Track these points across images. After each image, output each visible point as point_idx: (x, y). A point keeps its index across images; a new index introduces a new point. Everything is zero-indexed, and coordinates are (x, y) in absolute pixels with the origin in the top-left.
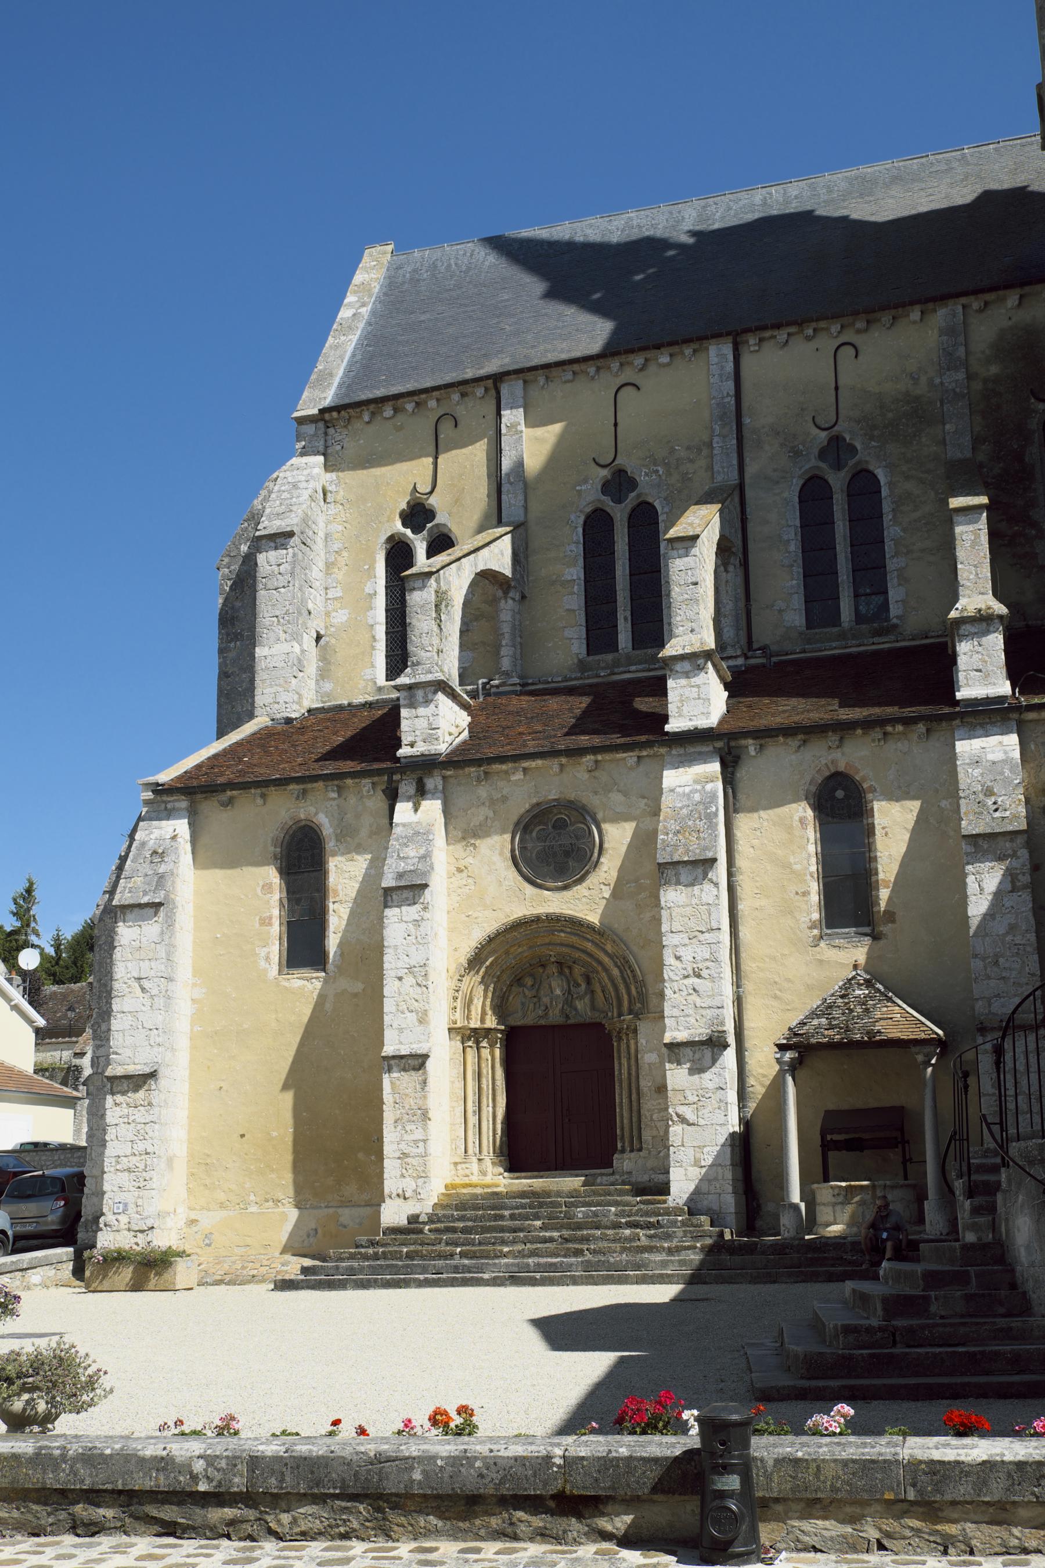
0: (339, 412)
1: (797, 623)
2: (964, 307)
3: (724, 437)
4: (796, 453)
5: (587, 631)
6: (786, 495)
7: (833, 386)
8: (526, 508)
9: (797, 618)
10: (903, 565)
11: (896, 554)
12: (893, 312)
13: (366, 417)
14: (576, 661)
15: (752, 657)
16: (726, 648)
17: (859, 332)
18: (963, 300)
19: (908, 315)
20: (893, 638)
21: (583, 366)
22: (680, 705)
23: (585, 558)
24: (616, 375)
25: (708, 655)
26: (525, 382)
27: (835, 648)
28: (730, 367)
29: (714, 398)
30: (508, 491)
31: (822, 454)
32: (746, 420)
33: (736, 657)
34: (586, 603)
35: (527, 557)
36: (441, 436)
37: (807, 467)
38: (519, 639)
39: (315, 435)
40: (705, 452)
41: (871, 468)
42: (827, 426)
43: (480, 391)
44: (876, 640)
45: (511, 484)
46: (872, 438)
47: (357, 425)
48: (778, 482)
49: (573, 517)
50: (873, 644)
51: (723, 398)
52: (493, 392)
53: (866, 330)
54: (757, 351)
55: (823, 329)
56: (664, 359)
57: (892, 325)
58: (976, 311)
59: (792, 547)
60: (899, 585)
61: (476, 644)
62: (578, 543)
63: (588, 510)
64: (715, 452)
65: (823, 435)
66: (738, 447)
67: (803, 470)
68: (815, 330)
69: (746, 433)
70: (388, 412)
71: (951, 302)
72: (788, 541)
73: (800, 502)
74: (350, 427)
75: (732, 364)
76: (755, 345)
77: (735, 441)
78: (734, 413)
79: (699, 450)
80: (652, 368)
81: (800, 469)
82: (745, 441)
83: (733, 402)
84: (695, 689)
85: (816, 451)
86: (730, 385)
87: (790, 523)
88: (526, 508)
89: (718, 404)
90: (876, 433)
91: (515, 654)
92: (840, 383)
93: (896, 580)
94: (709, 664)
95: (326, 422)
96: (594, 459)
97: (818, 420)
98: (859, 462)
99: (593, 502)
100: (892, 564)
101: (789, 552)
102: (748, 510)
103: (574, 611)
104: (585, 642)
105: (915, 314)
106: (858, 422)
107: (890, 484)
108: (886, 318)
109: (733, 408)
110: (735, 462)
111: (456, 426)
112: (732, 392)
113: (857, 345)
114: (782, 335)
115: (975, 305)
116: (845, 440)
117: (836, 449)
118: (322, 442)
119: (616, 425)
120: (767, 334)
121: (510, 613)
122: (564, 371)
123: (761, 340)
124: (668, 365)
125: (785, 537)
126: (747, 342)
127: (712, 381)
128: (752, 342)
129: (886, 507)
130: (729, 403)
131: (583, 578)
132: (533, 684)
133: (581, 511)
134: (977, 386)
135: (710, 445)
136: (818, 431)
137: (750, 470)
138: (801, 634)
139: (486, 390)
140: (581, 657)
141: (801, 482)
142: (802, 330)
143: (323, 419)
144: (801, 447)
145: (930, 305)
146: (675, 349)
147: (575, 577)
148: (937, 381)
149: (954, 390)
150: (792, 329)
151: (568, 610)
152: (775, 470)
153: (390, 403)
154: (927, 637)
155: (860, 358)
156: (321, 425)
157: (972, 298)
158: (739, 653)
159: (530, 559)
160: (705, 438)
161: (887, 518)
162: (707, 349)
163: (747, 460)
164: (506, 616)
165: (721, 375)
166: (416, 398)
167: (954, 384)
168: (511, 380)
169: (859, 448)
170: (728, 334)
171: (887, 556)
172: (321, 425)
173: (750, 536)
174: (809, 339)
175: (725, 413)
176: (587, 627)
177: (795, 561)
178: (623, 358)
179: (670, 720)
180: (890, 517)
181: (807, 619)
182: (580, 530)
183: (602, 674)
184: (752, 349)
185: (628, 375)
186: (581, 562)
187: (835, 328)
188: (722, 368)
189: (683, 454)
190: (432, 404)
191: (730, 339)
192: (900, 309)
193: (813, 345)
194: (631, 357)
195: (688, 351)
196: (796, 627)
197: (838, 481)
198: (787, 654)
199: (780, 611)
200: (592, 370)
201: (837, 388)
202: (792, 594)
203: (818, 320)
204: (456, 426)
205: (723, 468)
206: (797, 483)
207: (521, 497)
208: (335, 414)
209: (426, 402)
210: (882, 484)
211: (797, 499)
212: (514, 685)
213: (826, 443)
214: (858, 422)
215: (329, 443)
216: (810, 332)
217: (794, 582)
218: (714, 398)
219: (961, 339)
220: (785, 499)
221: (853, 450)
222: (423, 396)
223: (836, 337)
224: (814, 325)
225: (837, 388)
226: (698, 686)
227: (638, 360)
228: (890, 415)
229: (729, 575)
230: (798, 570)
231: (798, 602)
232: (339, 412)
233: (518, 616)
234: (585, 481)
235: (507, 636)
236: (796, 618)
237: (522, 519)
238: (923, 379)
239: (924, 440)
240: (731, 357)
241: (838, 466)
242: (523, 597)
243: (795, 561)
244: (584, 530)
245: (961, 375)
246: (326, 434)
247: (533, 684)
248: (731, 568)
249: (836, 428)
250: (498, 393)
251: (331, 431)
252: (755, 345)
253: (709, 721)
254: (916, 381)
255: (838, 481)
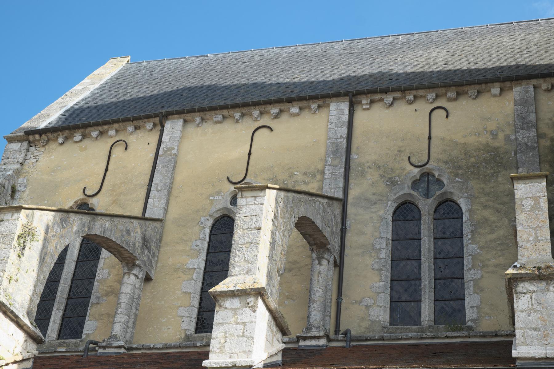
0: (41, 136)
1: (381, 318)
2: (535, 87)
3: (335, 166)
4: (392, 183)
5: (199, 312)
6: (381, 213)
7: (427, 136)
8: (166, 211)
9: (382, 313)
10: (479, 276)
11: (473, 267)
12: (478, 87)
13: (60, 140)
14: (183, 336)
15: (334, 340)
16: (311, 329)
17: (450, 100)
18: (534, 82)
19: (490, 91)
20: (465, 333)
21: (231, 112)
22: (222, 341)
23: (207, 253)
24: (256, 120)
25: (260, 293)
26: (185, 121)
27: (411, 338)
28: (345, 118)
29: (330, 138)
30: (155, 196)
31: (415, 184)
32: (354, 156)
33: (319, 338)
34: (202, 289)
35: (158, 248)
36: (113, 156)
37: (401, 193)
38: (134, 310)
39: (19, 151)
40: (318, 177)
41: (455, 198)
42: (420, 164)
43: (149, 125)
44: (449, 334)
45: (158, 191)
46: (457, 175)
47: (53, 146)
48: (375, 203)
49: (203, 220)
50: (447, 337)
51: (337, 139)
52: (159, 128)
53: (456, 99)
54: (368, 109)
55: (421, 97)
56: (295, 110)
57: (477, 96)
58: (545, 91)
59: (383, 255)
60: (475, 293)
61: (102, 315)
62: (204, 240)
63: (217, 215)
64: (326, 177)
65: (417, 170)
66: (345, 175)
67: (397, 195)
68: (415, 97)
69: (353, 165)
70: (78, 137)
71: (524, 82)
72: (380, 250)
73: (393, 221)
74: (47, 147)
75: (347, 116)
76: (367, 104)
77: (343, 170)
78: (345, 150)
79: (314, 176)
80: (285, 117)
81: (395, 194)
82: (351, 171)
83: (345, 142)
84: (241, 327)
85: (410, 183)
86: (345, 130)
87: (382, 235)
88: (166, 211)
89: (332, 143)
90: (460, 172)
91: (128, 322)
92: (433, 135)
93: (472, 289)
94: (260, 301)
95: (30, 142)
96: (228, 178)
97: (413, 160)
98: (445, 193)
99: (222, 209)
100: (469, 275)
101: (380, 259)
102: (348, 223)
103: (190, 293)
104: (195, 321)
105: (496, 90)
106: (446, 163)
107: (470, 211)
108: (472, 91)
109: (344, 147)
110: (341, 185)
111: (126, 149)
112: (345, 135)
113: (448, 109)
114: (389, 99)
115: (544, 86)
116: (433, 176)
117: (426, 180)
118: (23, 154)
119: (250, 154)
120: (377, 97)
121: (130, 287)
122: (216, 114)
123: (372, 102)
124: (297, 115)
125: (378, 246)
126: (360, 102)
127: (330, 126)
128: (364, 102)
129: (467, 229)
130: (341, 142)
131: (203, 267)
132: (137, 349)
133: (210, 216)
134: (545, 143)
135: (323, 173)
136: (412, 168)
137: (353, 193)
138: (384, 328)
139: (155, 125)
140: (188, 333)
141: (396, 205)
142: (405, 96)
143: (28, 140)
144: (397, 178)
145: (508, 84)
146: (304, 104)
147: (195, 267)
148: (513, 137)
149: (526, 144)
150: (398, 95)
151: (185, 293)
152: (374, 194)
153: (81, 131)
154: (496, 336)
155: (449, 118)
156: (25, 144)
157: (541, 81)
158: (322, 334)
159: (161, 250)
160: (320, 167)
161: (467, 237)
162: (329, 106)
163: (352, 185)
164: (127, 289)
165: (337, 123)
166: (100, 128)
167: (526, 140)
168: (174, 119)
169: (445, 182)
170: (346, 94)
171: (465, 268)
172: (25, 144)
173: (347, 243)
174: (410, 103)
175: (337, 150)
176: (200, 308)
177: (384, 266)
178: (263, 108)
179: (211, 356)
180: (469, 237)
181: (391, 316)
182: (208, 231)
183: (198, 345)
184: (364, 107)
185: (265, 121)
186: (204, 255)
187: (431, 96)
188: (339, 118)
189: (300, 177)
190: (112, 132)
191: (347, 98)
192: (483, 85)
193: (413, 107)
194: (269, 107)
195: (314, 106)
196: (380, 321)
197: (426, 206)
198: (366, 340)
199: (367, 307)
200: (237, 115)
201: (430, 138)
202: (379, 293)
203: (417, 89)
204: (126, 149)
205: (331, 189)
206: (391, 207)
207: (164, 201)
208: (37, 137)
209: (107, 132)
210: (464, 211)
211: (390, 218)
212: (119, 347)
213: (418, 177)
214: (446, 163)
215: (29, 157)
216: (411, 97)
217: (382, 283)
218: (330, 138)
219: (533, 108)
220: (381, 217)
221: (440, 183)
222: (106, 127)
223: (432, 103)
224: (414, 92)
225: (430, 138)
226: (244, 324)
227: (275, 110)
228: (473, 160)
229: (322, 267)
230: (387, 274)
231: (384, 300)
232: (41, 136)
233: (137, 291)
234: (218, 193)
235: (123, 305)
236: (381, 314)
237: (161, 217)
238: (501, 136)
239: (500, 179)
240: (347, 111)
241: (427, 195)
242: (148, 279)
243: (384, 266)
244: (211, 231)
245: (532, 133)
246: (28, 151)
247: (137, 349)
248: (325, 262)
249: (427, 166)
250: (163, 127)
251: (32, 149)
252: (367, 104)
253: (249, 360)
254: (494, 135)
255: (426, 206)
